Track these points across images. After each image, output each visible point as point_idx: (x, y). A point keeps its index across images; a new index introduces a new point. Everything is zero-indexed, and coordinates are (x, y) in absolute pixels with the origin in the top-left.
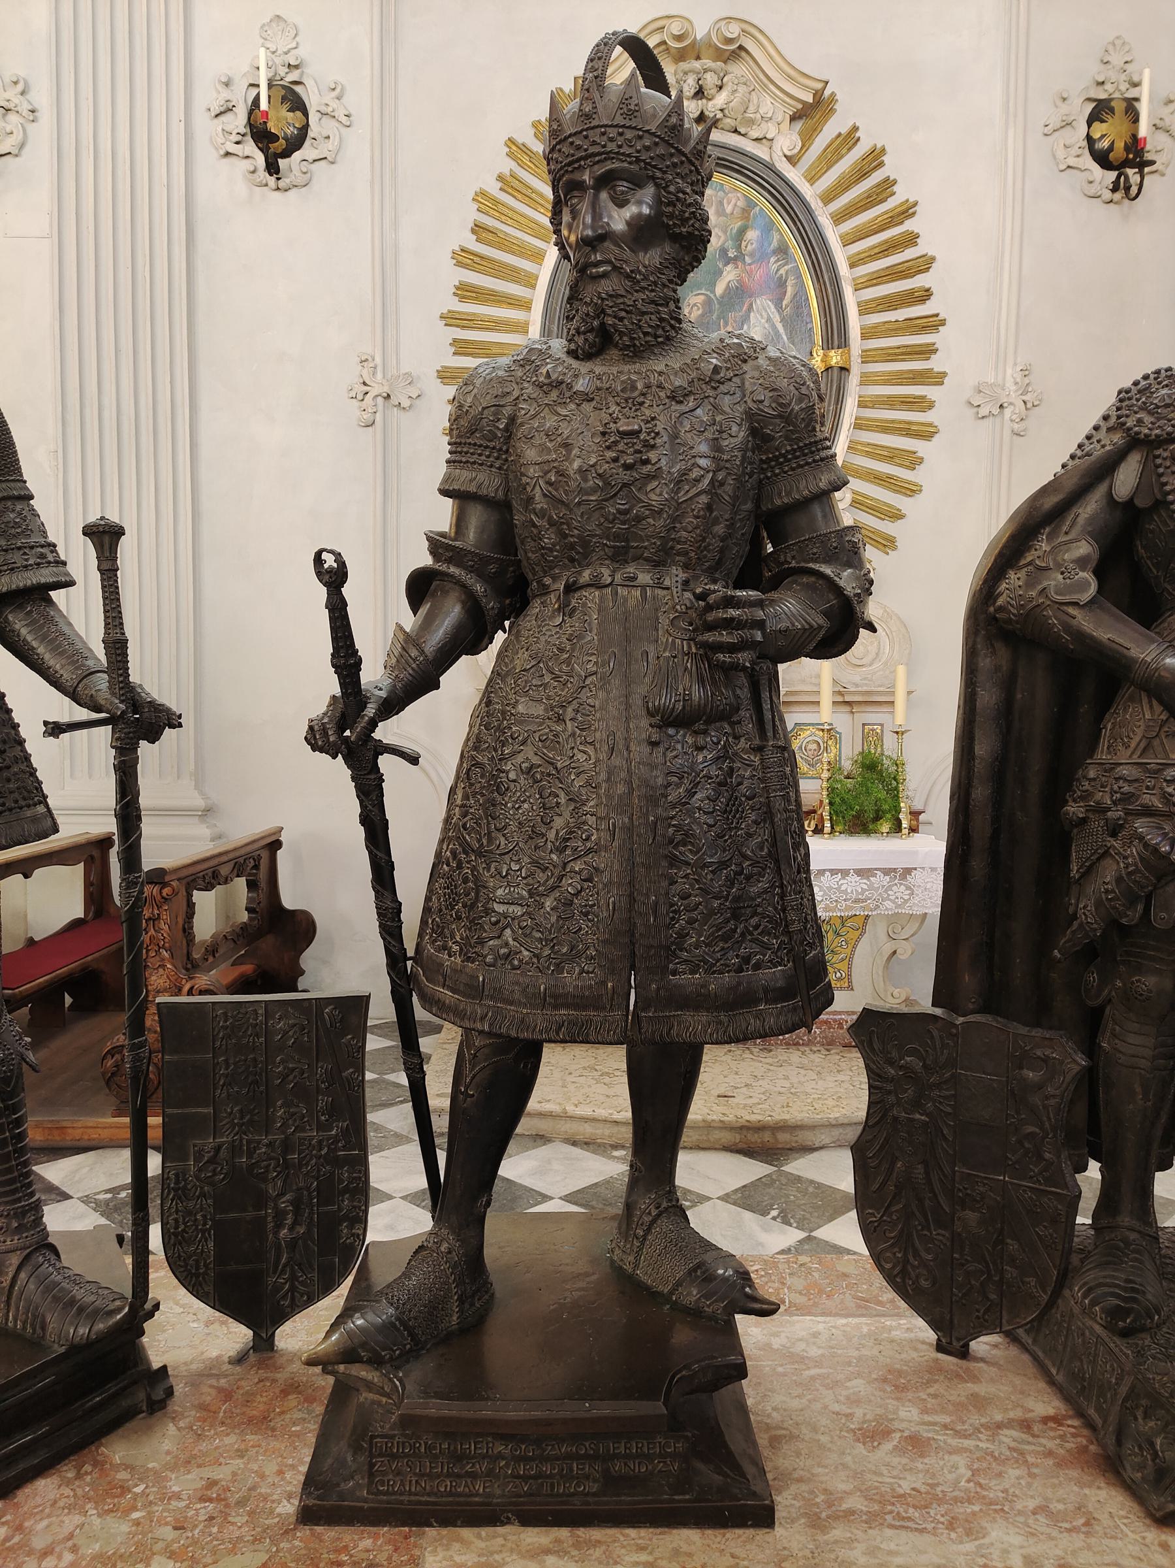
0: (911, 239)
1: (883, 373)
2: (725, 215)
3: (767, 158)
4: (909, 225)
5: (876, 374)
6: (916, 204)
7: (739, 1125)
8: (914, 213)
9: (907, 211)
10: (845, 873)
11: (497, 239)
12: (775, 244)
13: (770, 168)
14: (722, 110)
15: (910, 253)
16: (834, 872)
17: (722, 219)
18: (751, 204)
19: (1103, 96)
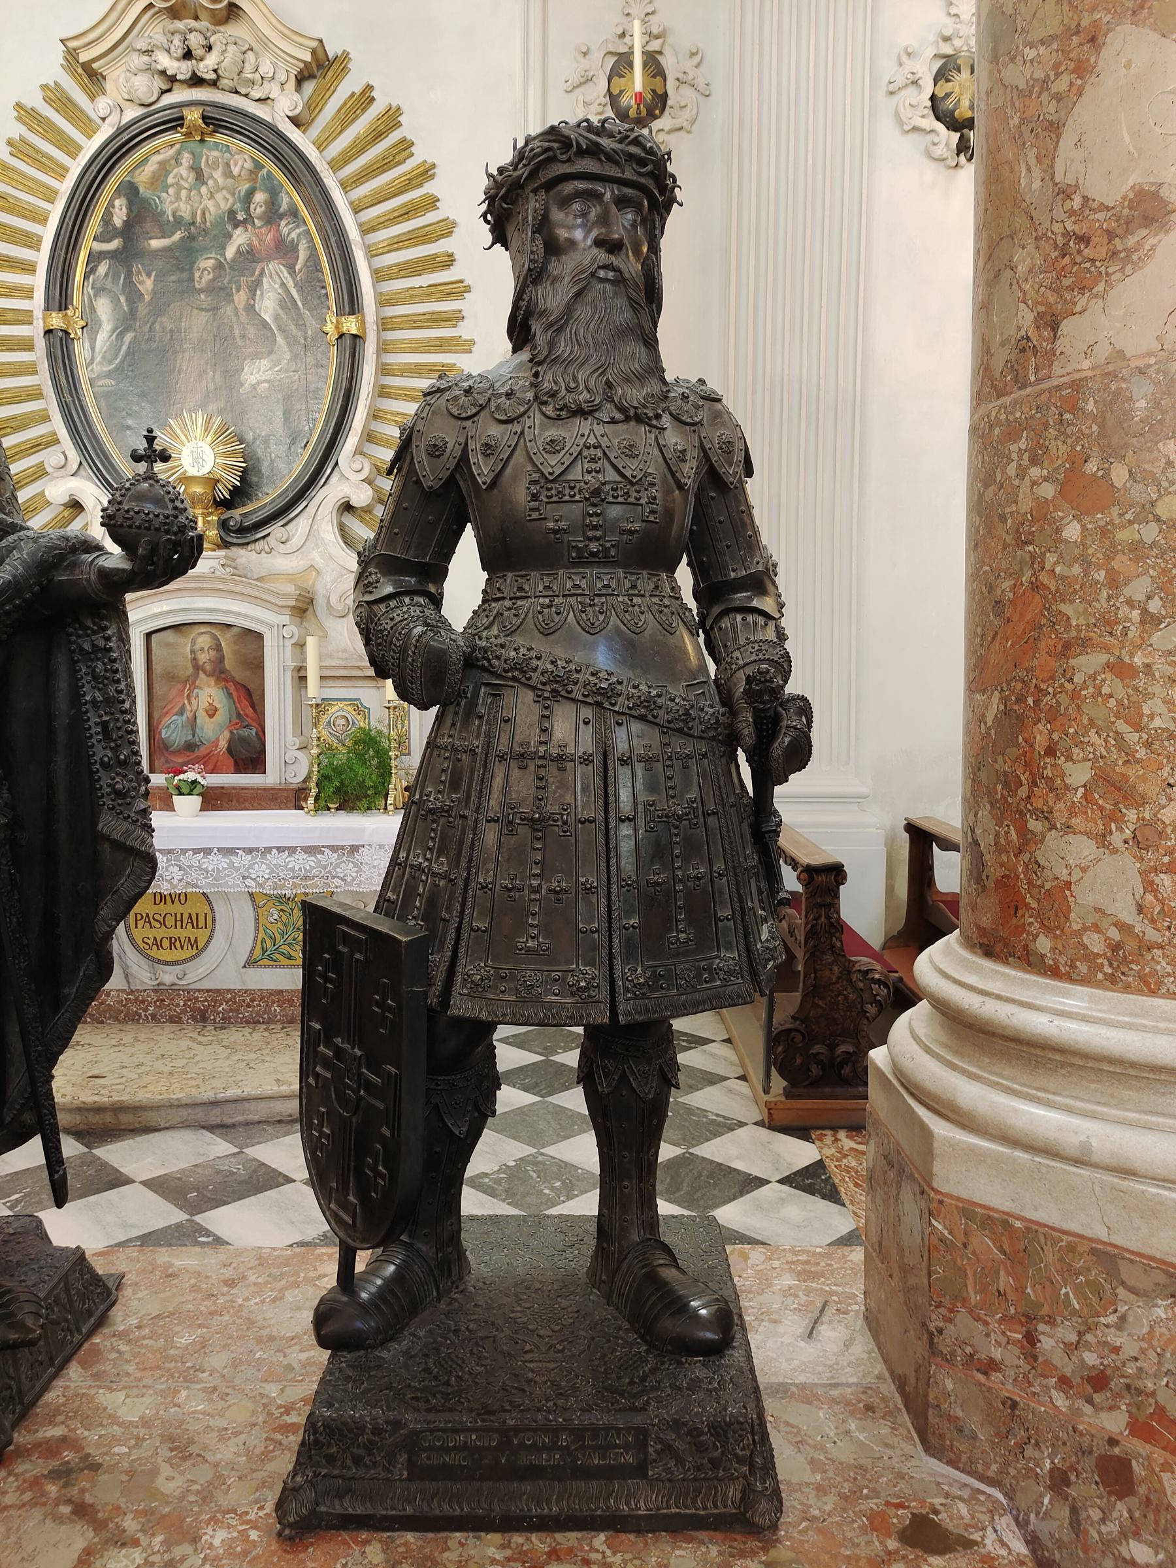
0: (432, 203)
1: (411, 341)
2: (233, 177)
3: (270, 120)
4: (429, 188)
5: (403, 341)
6: (434, 166)
7: (74, 1106)
8: (433, 175)
9: (426, 173)
10: (292, 850)
11: (8, 205)
12: (284, 207)
13: (272, 129)
14: (215, 71)
15: (431, 217)
16: (280, 850)
17: (230, 181)
18: (258, 166)
19: (950, 51)
